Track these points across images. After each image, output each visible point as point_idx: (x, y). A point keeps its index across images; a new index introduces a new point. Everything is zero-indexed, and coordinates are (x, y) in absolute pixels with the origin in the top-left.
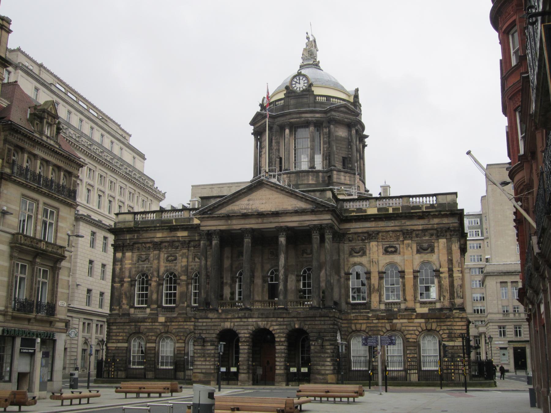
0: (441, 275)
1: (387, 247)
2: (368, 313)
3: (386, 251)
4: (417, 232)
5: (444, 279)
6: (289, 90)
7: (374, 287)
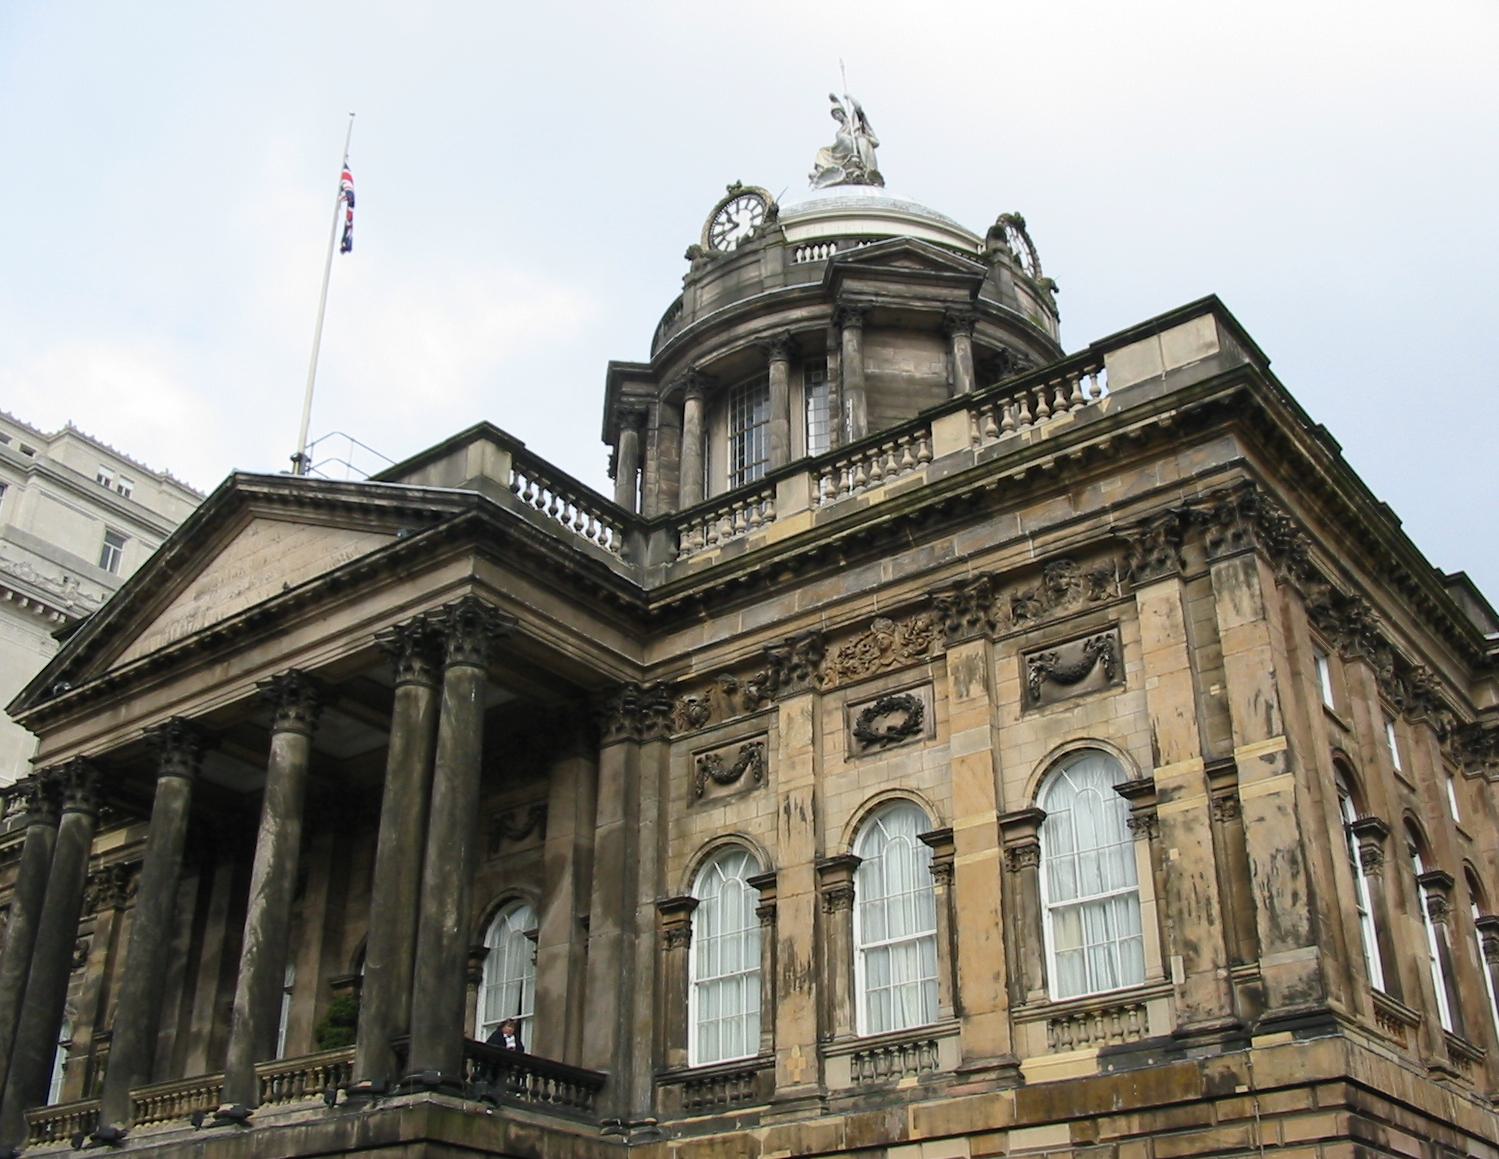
0: (1163, 811)
1: (869, 716)
2: (753, 1121)
3: (867, 740)
4: (1021, 590)
5: (1180, 834)
6: (706, 263)
7: (792, 957)
